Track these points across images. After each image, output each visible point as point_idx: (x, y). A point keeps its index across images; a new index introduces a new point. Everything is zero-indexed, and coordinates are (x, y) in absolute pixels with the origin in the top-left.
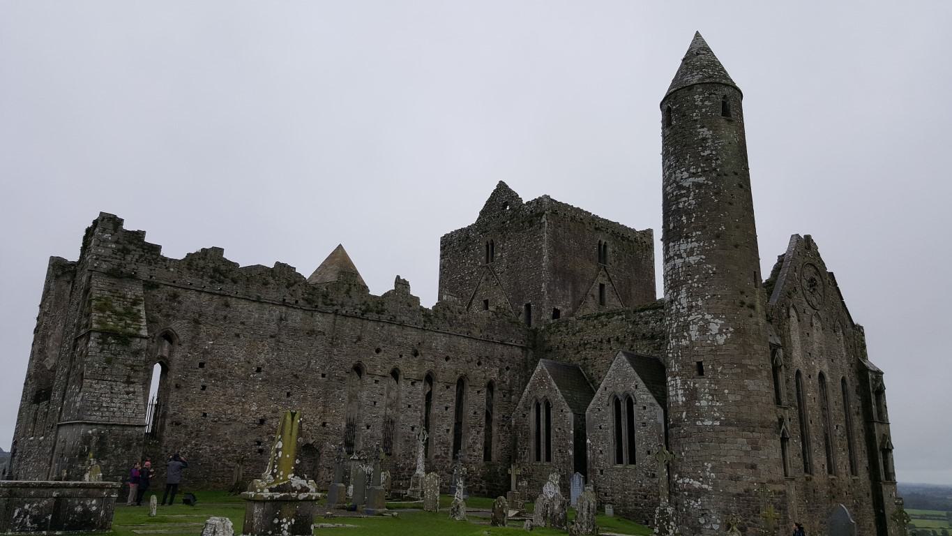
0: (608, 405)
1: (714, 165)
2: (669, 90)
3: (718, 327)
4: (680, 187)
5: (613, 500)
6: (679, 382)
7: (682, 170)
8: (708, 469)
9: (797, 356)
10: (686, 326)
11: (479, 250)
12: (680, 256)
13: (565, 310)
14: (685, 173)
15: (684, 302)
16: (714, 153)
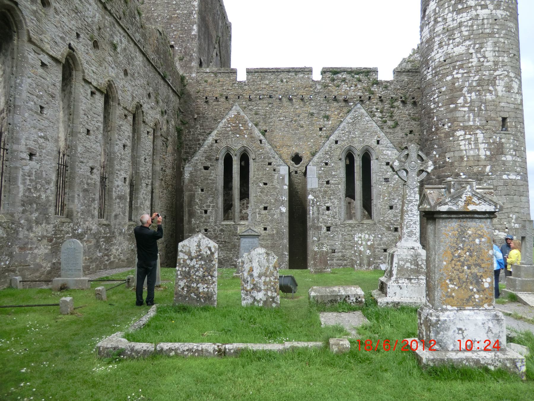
0: (340, 159)
5: (343, 256)
8: (513, 221)
10: (492, 81)
15: (489, 55)
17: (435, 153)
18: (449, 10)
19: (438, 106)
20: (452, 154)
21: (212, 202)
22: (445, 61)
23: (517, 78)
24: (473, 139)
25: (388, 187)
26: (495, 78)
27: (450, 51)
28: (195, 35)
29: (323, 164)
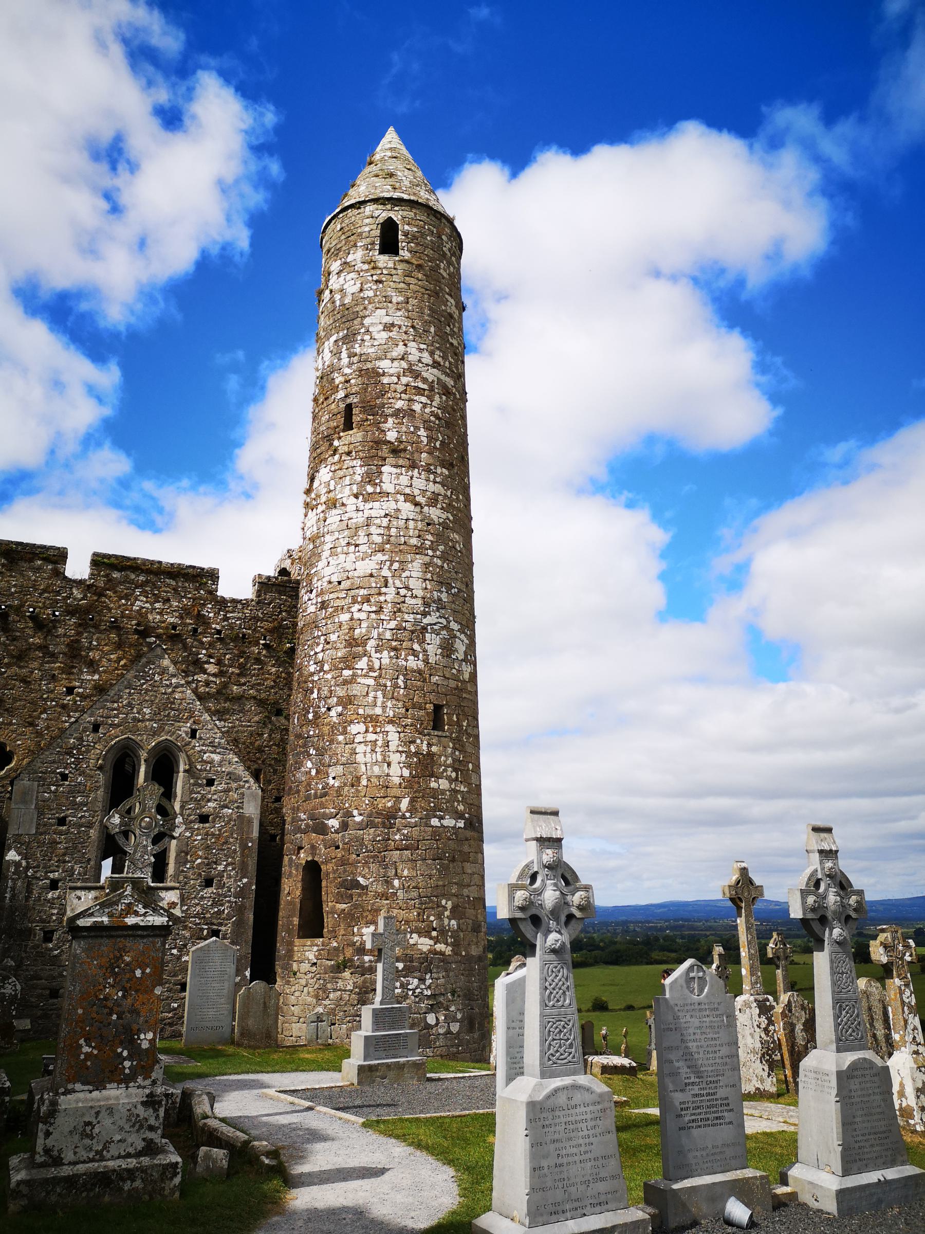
4: (417, 375)
7: (422, 346)
8: (447, 913)
14: (426, 354)
17: (309, 764)
18: (351, 489)
19: (322, 670)
20: (339, 769)
22: (339, 583)
23: (464, 633)
24: (379, 743)
26: (424, 629)
27: (349, 566)
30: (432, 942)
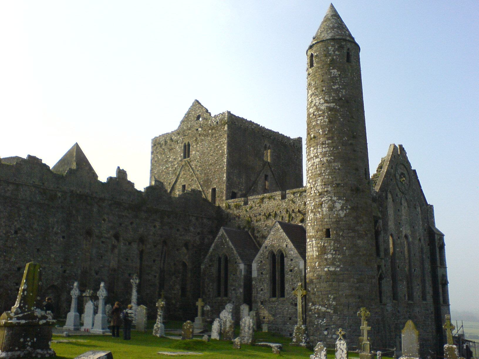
1: (340, 95)
2: (312, 42)
3: (341, 206)
6: (314, 242)
7: (320, 98)
8: (331, 300)
9: (391, 224)
11: (179, 149)
12: (317, 157)
13: (240, 193)
16: (341, 87)
21: (212, 286)
25: (292, 275)
28: (224, 180)
29: (259, 262)
30: (325, 309)
